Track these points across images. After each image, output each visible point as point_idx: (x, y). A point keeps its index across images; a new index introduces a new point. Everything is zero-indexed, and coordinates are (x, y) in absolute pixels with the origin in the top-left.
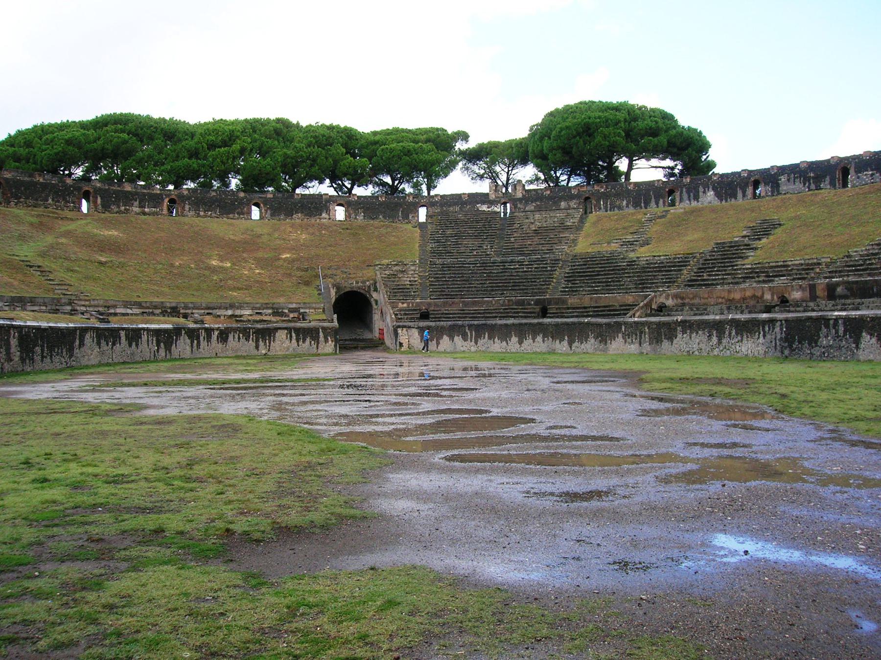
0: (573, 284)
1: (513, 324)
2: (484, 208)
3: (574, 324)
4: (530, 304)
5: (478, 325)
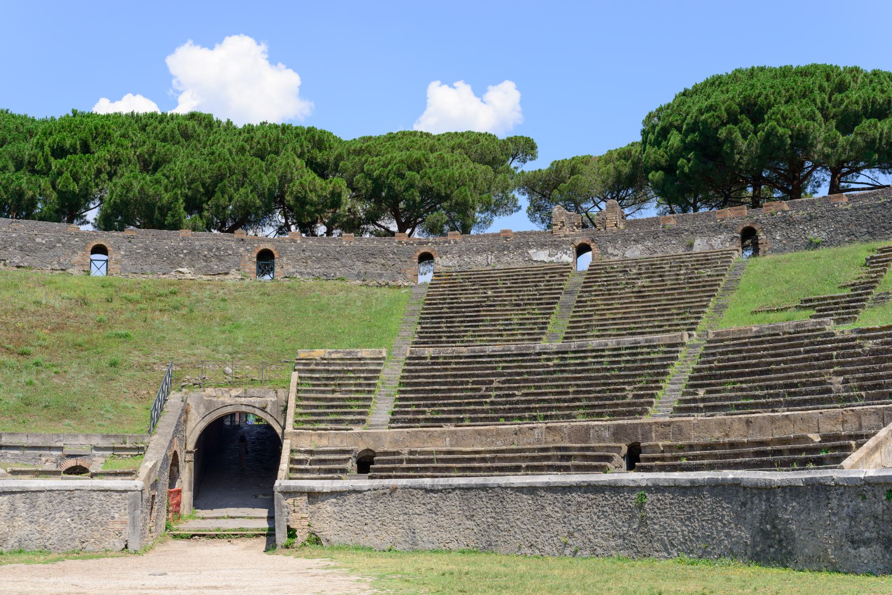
0: (708, 392)
2: (542, 256)
4: (600, 439)
5: (468, 489)
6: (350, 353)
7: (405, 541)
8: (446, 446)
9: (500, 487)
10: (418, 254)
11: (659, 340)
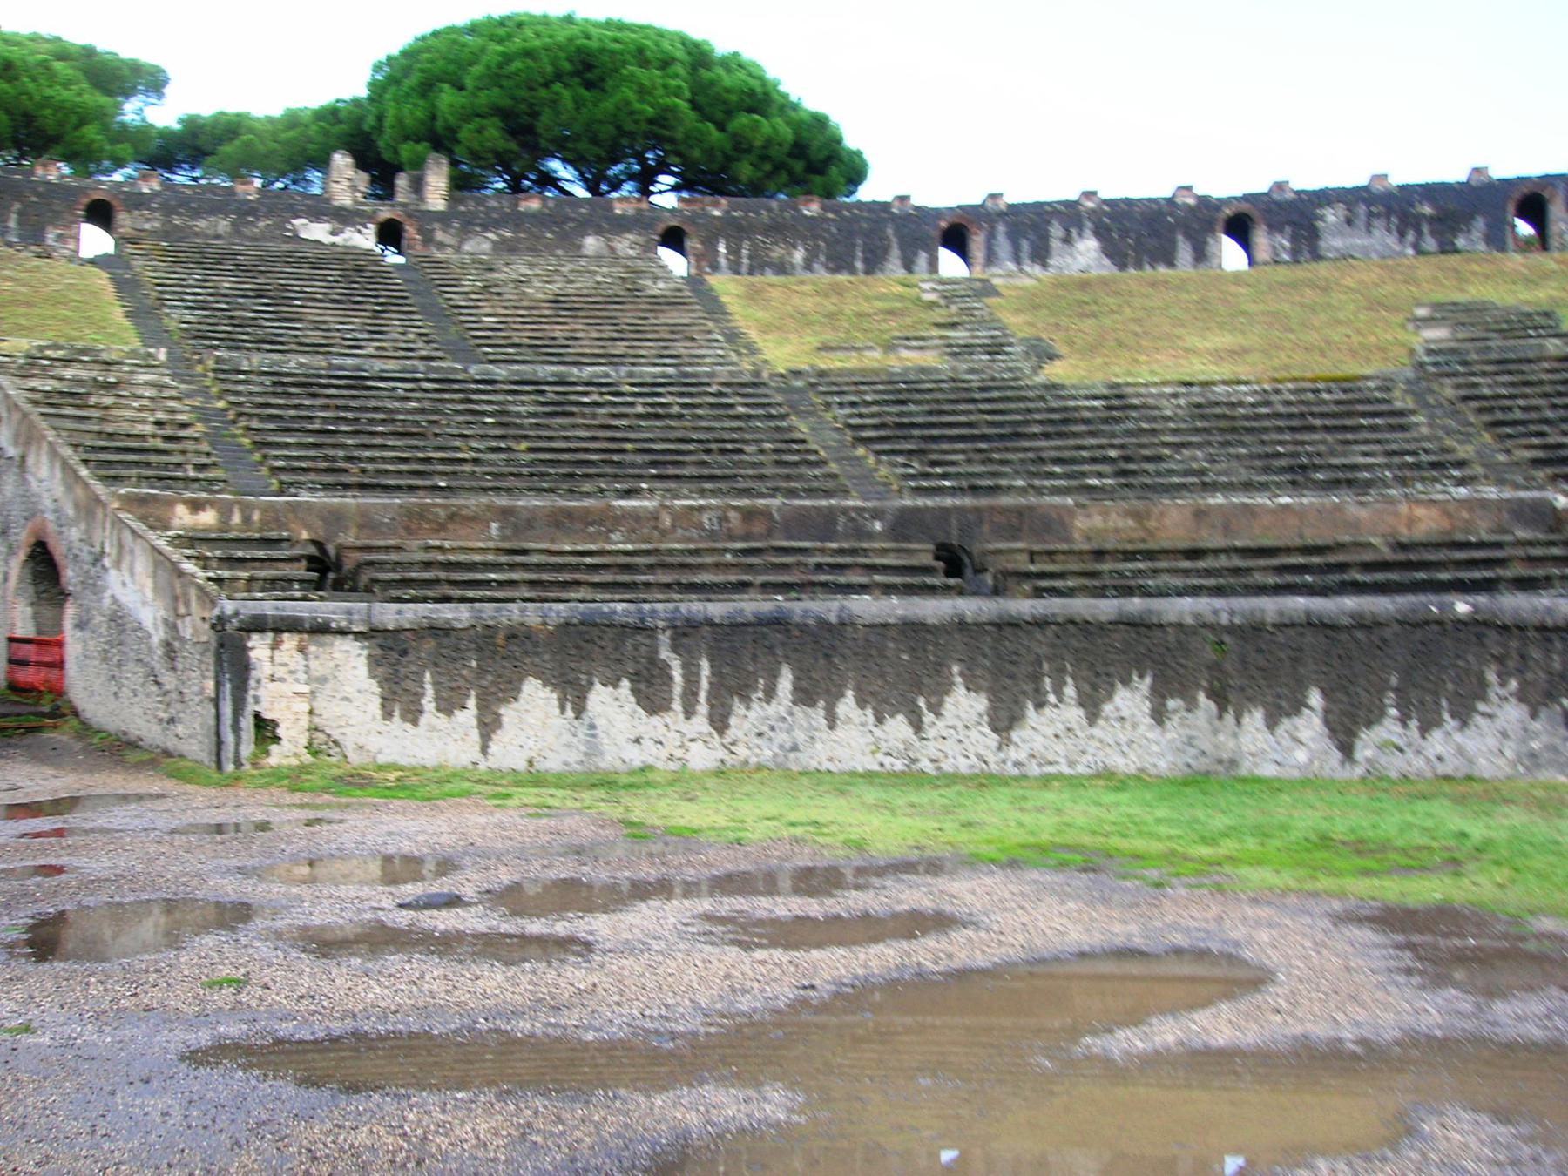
1: (962, 625)
2: (317, 231)
3: (1365, 624)
5: (735, 627)
6: (84, 351)
7: (568, 745)
8: (490, 539)
9: (823, 623)
10: (86, 201)
11: (711, 375)
